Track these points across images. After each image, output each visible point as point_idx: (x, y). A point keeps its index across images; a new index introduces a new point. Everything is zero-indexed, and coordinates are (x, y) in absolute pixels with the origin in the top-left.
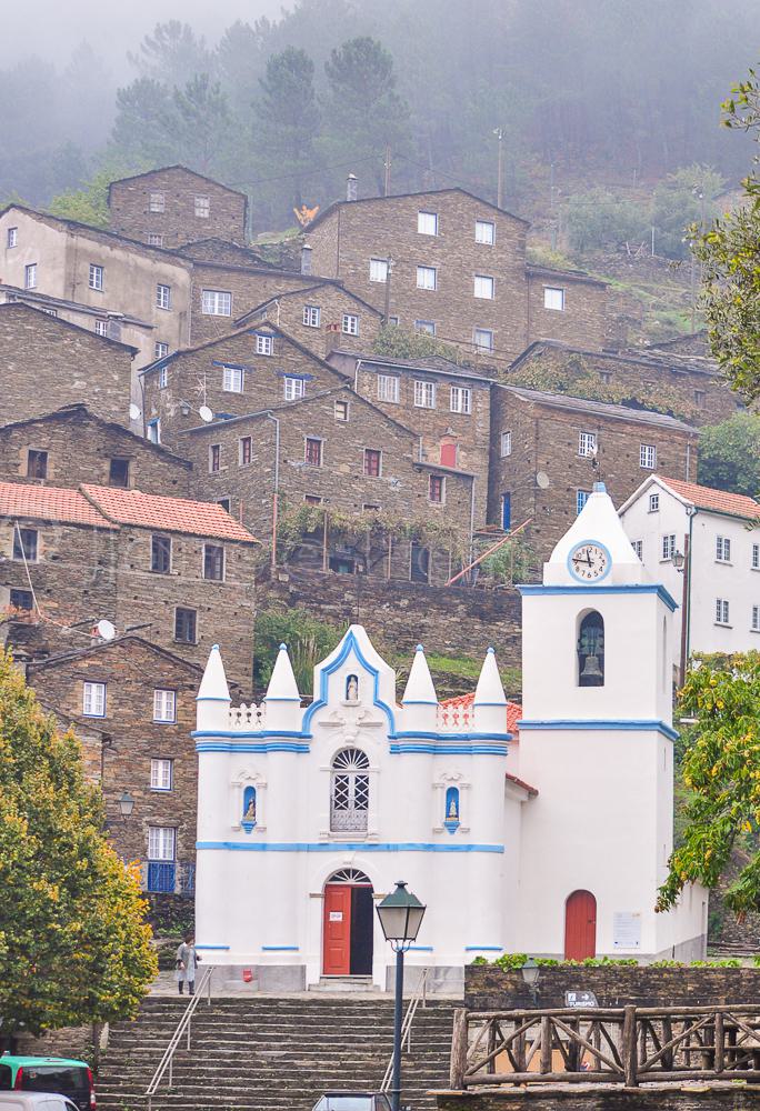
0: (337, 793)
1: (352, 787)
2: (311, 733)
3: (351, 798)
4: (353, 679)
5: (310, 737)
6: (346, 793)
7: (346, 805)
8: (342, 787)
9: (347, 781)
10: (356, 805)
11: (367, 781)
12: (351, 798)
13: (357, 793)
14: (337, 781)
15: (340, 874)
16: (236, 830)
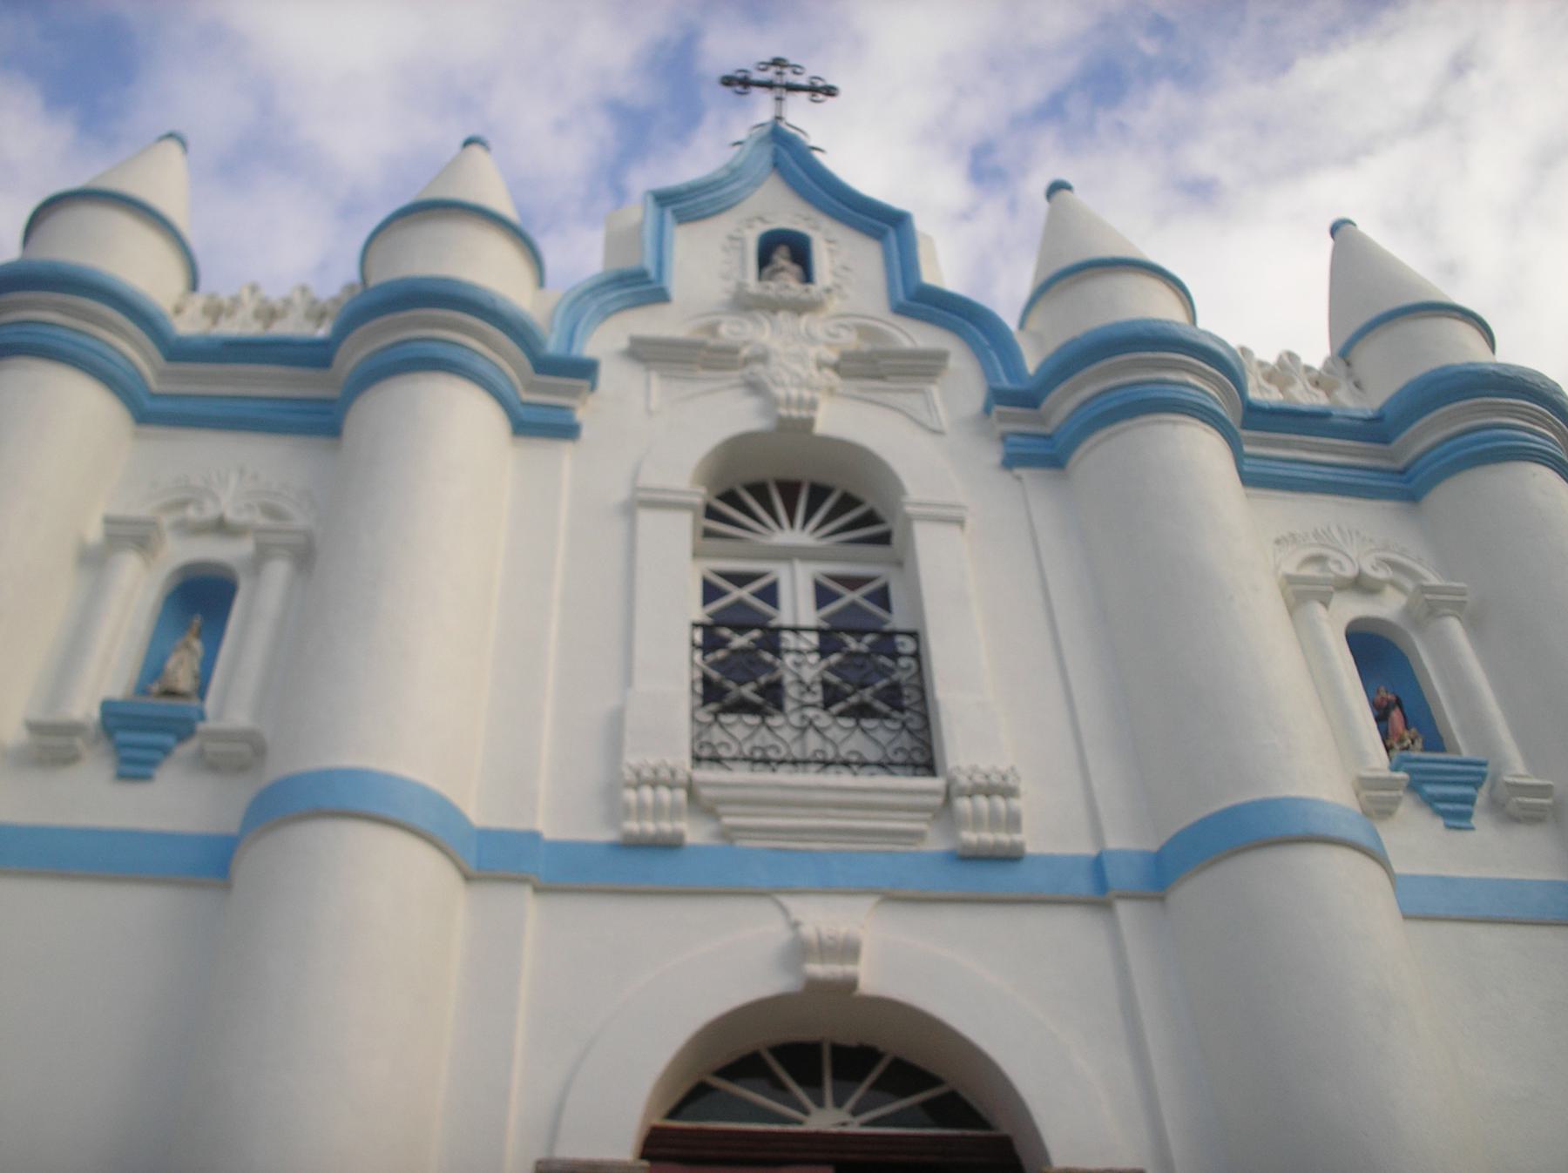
0: (710, 639)
3: (802, 665)
4: (781, 258)
5: (585, 370)
6: (772, 639)
7: (773, 695)
9: (770, 594)
10: (831, 695)
11: (882, 597)
12: (802, 665)
13: (828, 640)
15: (746, 1068)
16: (50, 745)
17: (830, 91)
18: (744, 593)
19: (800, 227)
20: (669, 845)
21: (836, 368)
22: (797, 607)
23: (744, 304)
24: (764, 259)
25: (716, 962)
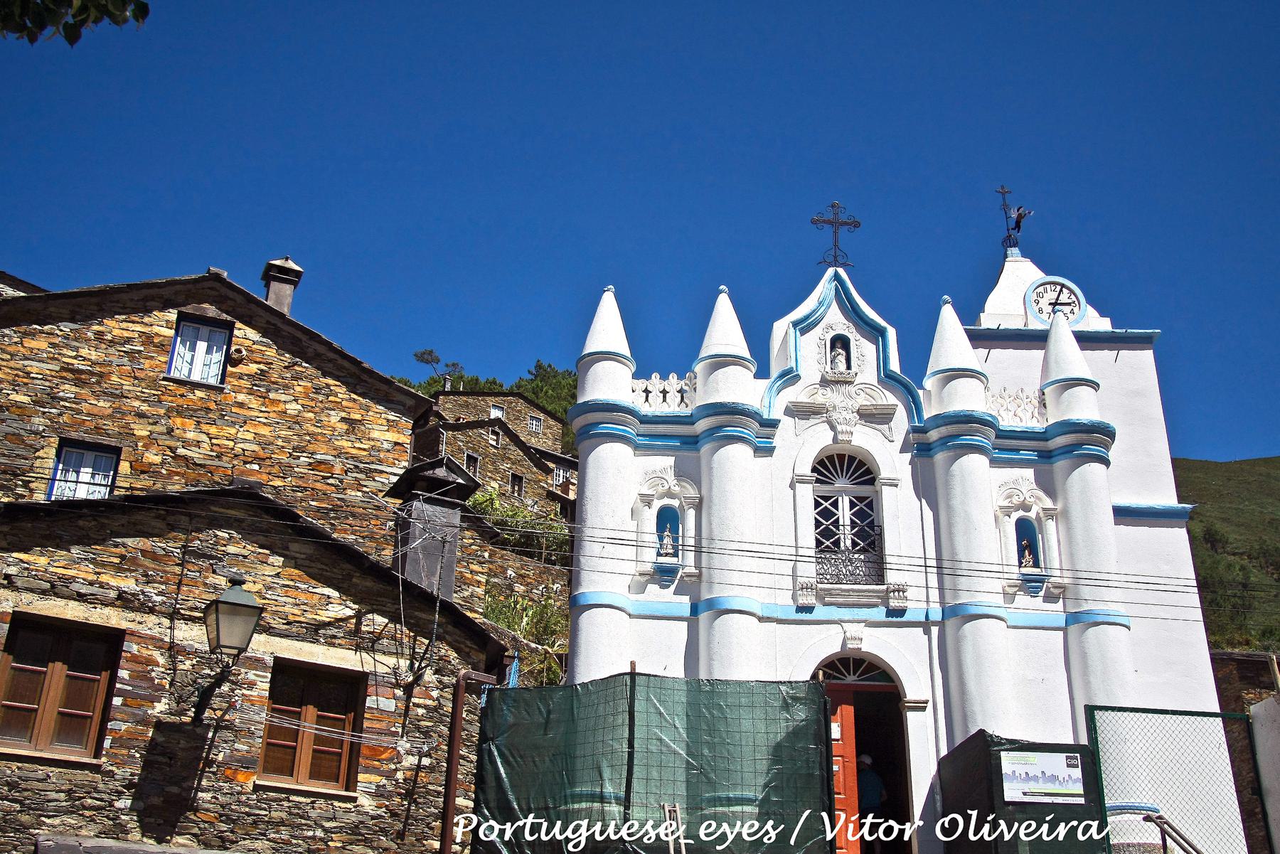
1: (845, 514)
2: (774, 416)
5: (773, 424)
7: (837, 543)
8: (826, 514)
9: (835, 504)
11: (870, 505)
14: (817, 504)
17: (857, 225)
18: (826, 504)
19: (846, 333)
20: (809, 609)
21: (858, 412)
22: (844, 502)
23: (825, 382)
24: (833, 348)
25: (822, 643)
